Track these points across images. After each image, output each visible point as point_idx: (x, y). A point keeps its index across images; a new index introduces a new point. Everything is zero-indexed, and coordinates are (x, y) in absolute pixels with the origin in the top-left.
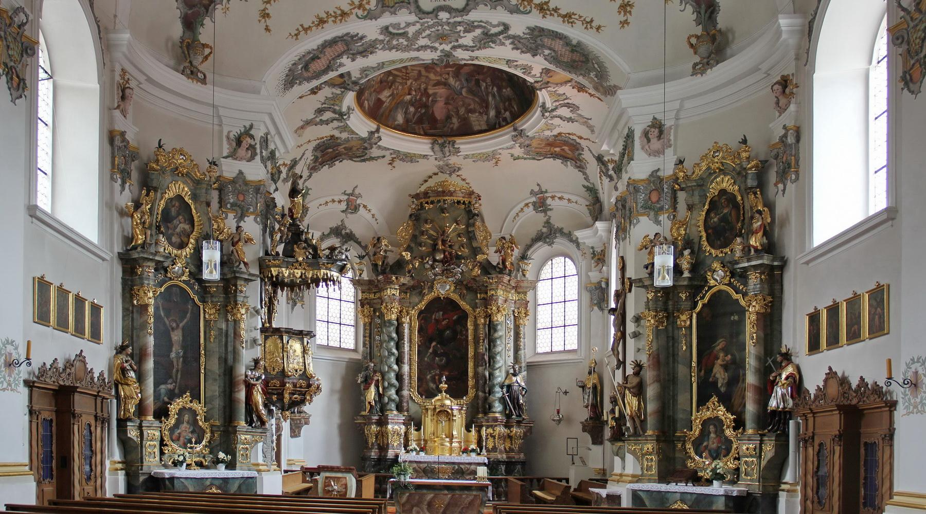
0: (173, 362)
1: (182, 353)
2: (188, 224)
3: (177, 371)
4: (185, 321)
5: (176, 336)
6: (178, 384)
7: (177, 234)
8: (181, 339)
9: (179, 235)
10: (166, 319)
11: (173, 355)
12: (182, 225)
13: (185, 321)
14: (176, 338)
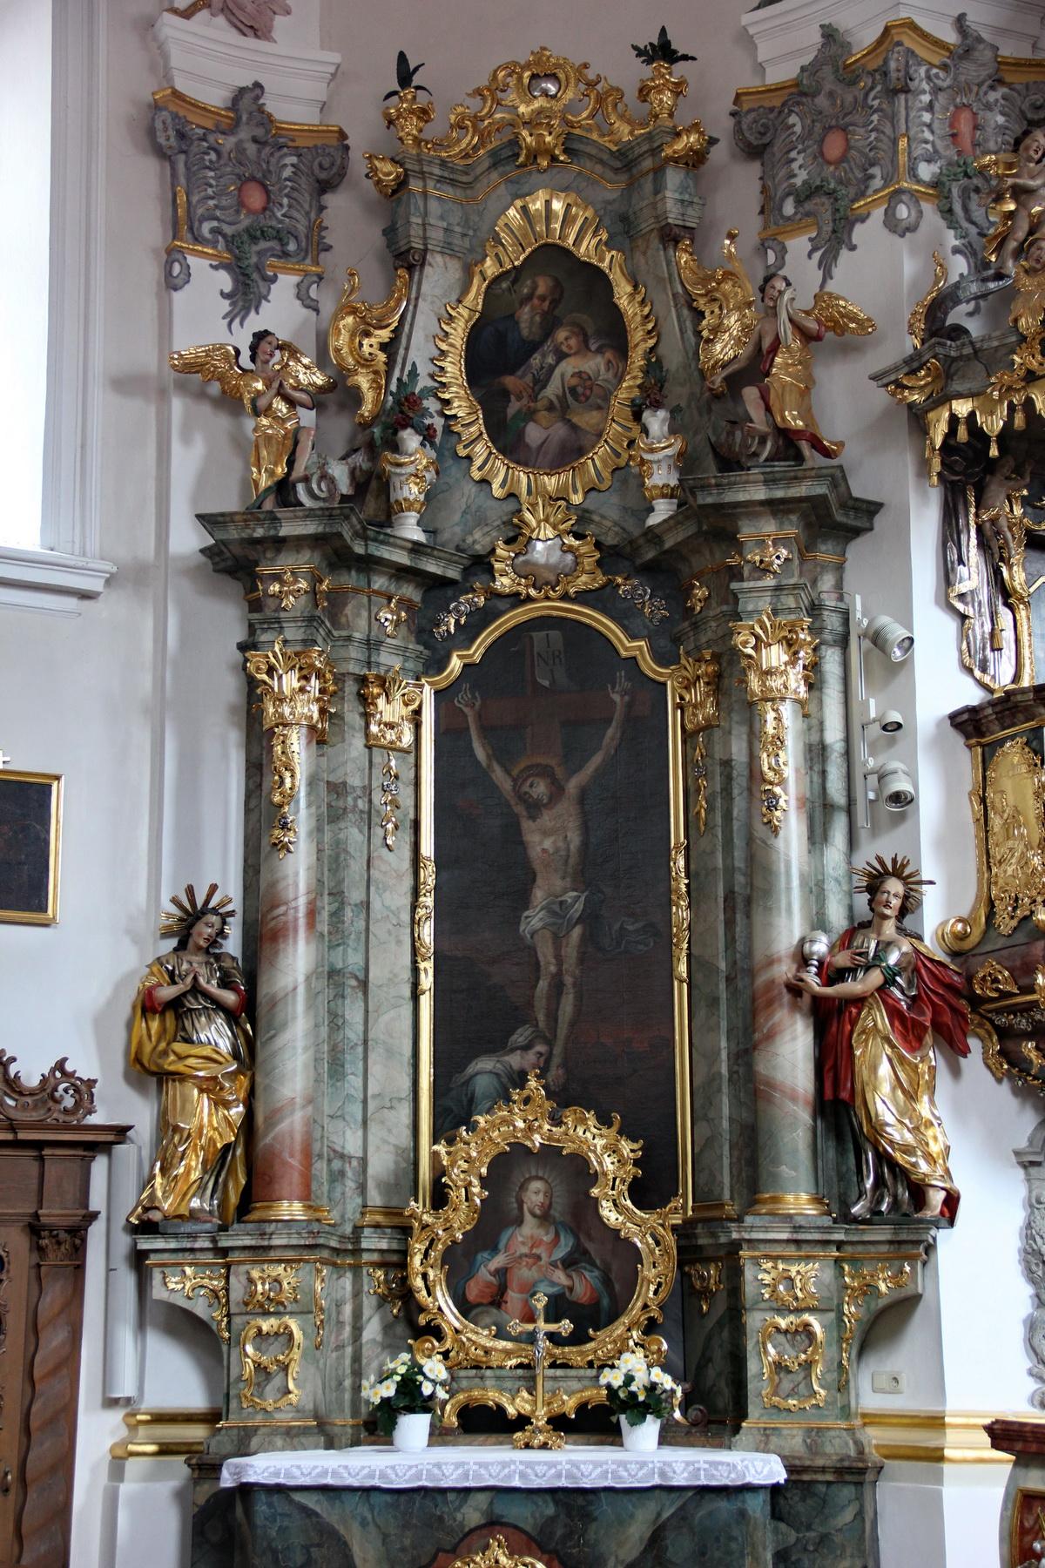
0: (532, 950)
1: (579, 906)
2: (599, 351)
3: (557, 987)
4: (596, 760)
5: (546, 833)
6: (557, 1050)
7: (550, 407)
8: (575, 839)
9: (560, 409)
10: (498, 775)
11: (534, 920)
12: (568, 367)
13: (596, 760)
14: (548, 844)
